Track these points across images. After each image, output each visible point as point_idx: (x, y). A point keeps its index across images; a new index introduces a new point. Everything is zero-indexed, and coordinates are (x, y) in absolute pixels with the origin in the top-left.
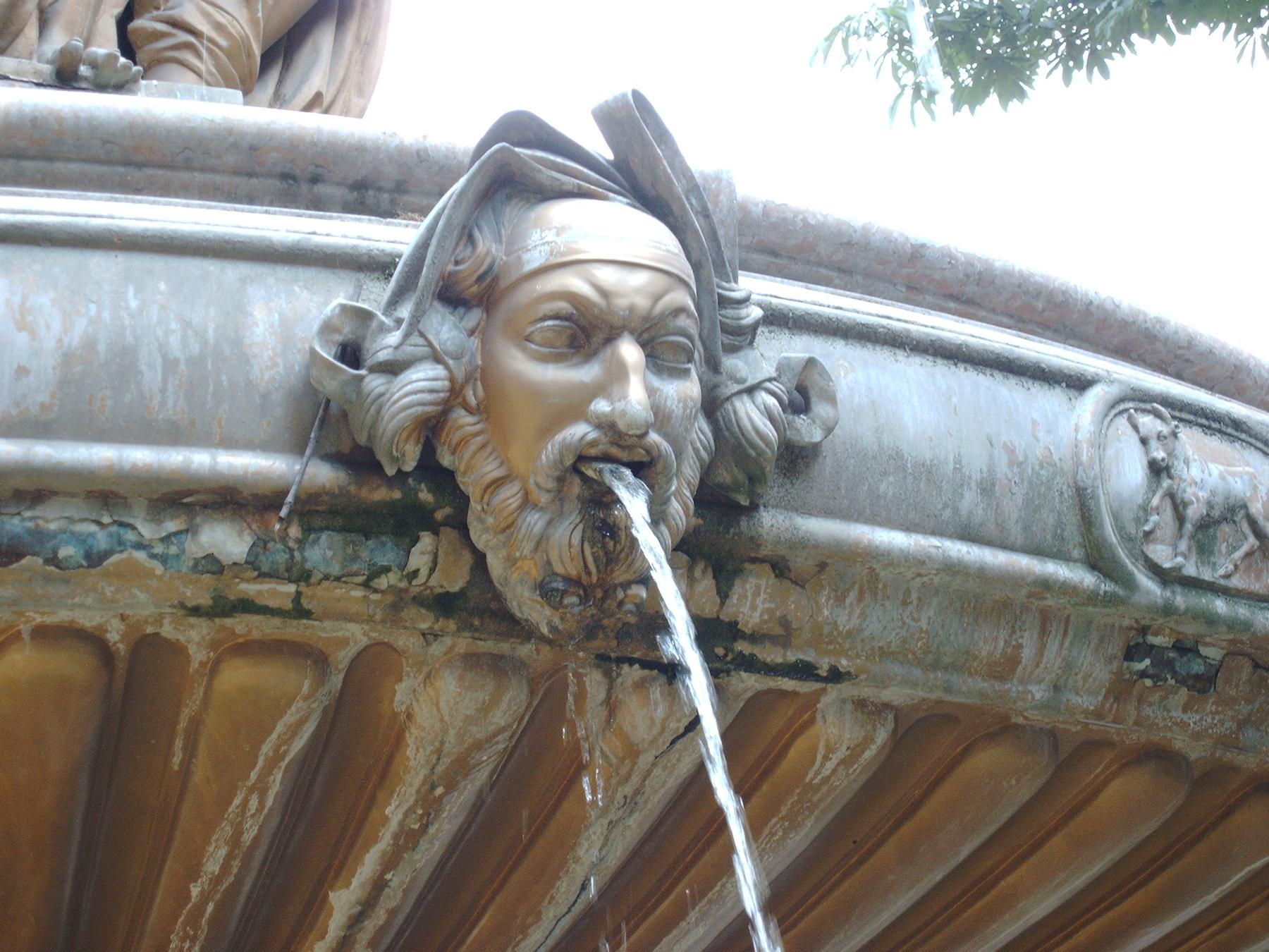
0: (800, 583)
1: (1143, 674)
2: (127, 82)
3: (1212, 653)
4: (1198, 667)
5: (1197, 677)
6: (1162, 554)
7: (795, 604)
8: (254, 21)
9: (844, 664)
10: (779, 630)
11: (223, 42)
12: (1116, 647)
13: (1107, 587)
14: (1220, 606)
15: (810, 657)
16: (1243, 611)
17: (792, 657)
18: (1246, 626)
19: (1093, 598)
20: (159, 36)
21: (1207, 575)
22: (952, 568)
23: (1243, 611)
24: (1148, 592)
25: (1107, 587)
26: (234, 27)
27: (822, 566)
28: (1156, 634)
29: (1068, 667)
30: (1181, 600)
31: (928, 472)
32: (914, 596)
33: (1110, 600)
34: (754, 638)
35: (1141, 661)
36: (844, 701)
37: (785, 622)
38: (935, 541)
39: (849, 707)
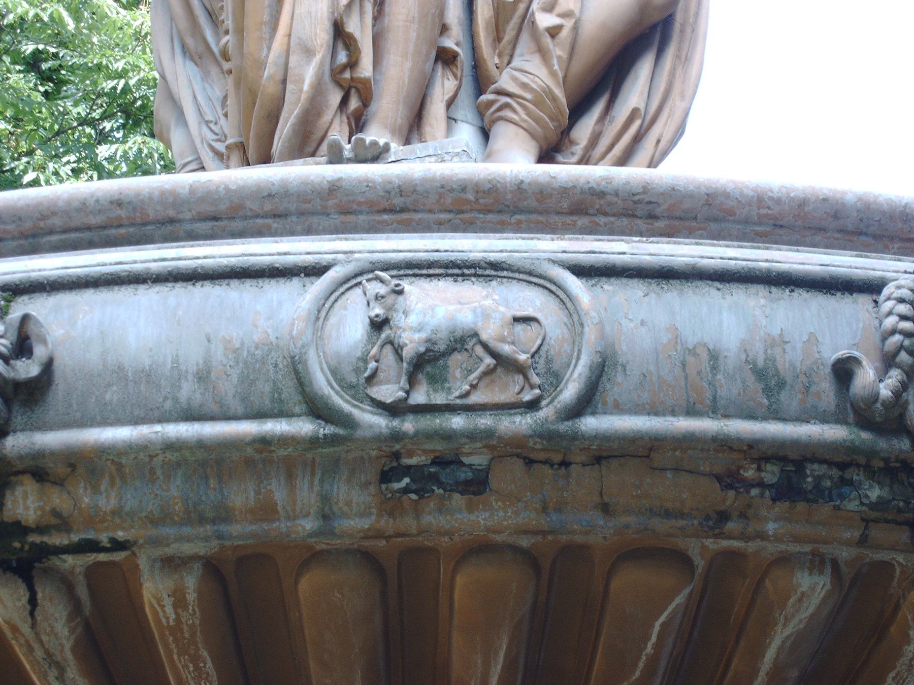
0: (59, 483)
1: (406, 491)
2: (381, 153)
3: (479, 460)
4: (464, 475)
5: (467, 483)
6: (388, 392)
7: (58, 499)
8: (553, 74)
9: (120, 535)
10: (54, 521)
11: (528, 96)
12: (371, 474)
13: (329, 430)
14: (458, 422)
15: (91, 535)
16: (485, 421)
17: (75, 538)
18: (489, 434)
19: (314, 442)
20: (491, 103)
21: (439, 399)
22: (172, 446)
23: (485, 421)
24: (371, 426)
25: (329, 430)
26: (535, 82)
27: (73, 466)
28: (410, 454)
29: (325, 499)
30: (408, 425)
31: (148, 376)
32: (159, 472)
33: (332, 440)
34: (41, 529)
35: (400, 480)
36: (154, 561)
37: (55, 513)
38: (158, 428)
39: (158, 565)
